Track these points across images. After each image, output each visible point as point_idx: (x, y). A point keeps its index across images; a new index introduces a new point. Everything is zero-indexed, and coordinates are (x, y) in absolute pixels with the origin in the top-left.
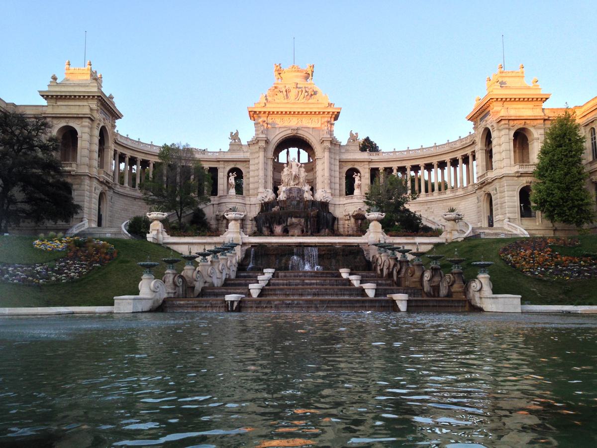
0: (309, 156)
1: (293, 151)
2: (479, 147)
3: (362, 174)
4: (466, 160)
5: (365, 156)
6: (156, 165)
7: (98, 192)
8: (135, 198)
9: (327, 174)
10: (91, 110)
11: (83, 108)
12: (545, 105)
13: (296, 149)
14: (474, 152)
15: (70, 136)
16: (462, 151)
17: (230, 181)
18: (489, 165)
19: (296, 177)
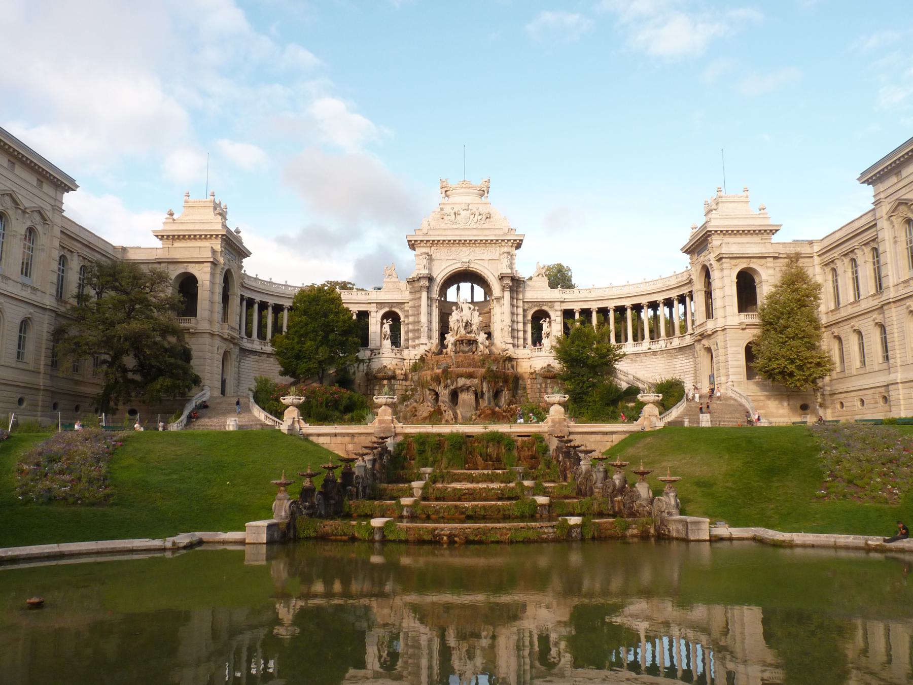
0: (485, 294)
1: (465, 286)
2: (698, 287)
3: (553, 317)
4: (682, 299)
5: (557, 294)
6: (291, 309)
7: (222, 351)
10: (214, 251)
12: (775, 238)
13: (469, 284)
14: (691, 292)
16: (677, 290)
17: (384, 330)
18: (709, 314)
19: (468, 324)
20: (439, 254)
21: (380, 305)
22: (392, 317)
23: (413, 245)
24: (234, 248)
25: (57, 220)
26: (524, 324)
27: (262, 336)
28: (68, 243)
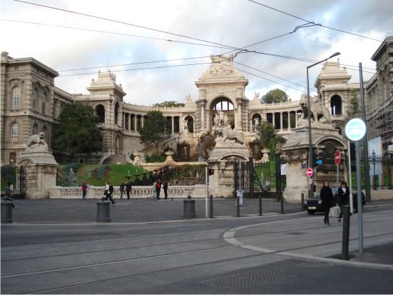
1: (225, 103)
6: (145, 117)
8: (136, 137)
9: (240, 118)
11: (105, 96)
12: (349, 82)
15: (101, 110)
20: (209, 90)
21: (184, 113)
22: (190, 120)
23: (198, 85)
24: (119, 93)
25: (52, 88)
26: (249, 120)
27: (132, 129)
28: (56, 97)
